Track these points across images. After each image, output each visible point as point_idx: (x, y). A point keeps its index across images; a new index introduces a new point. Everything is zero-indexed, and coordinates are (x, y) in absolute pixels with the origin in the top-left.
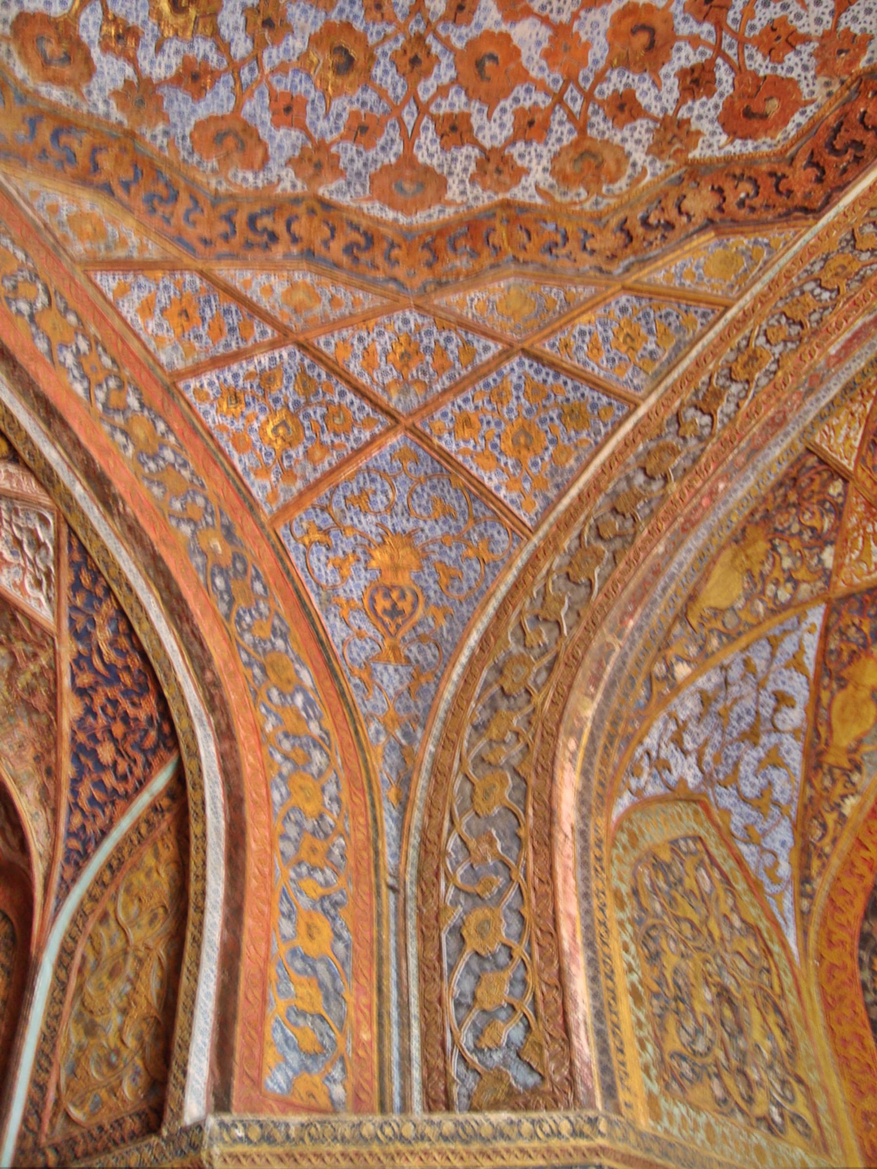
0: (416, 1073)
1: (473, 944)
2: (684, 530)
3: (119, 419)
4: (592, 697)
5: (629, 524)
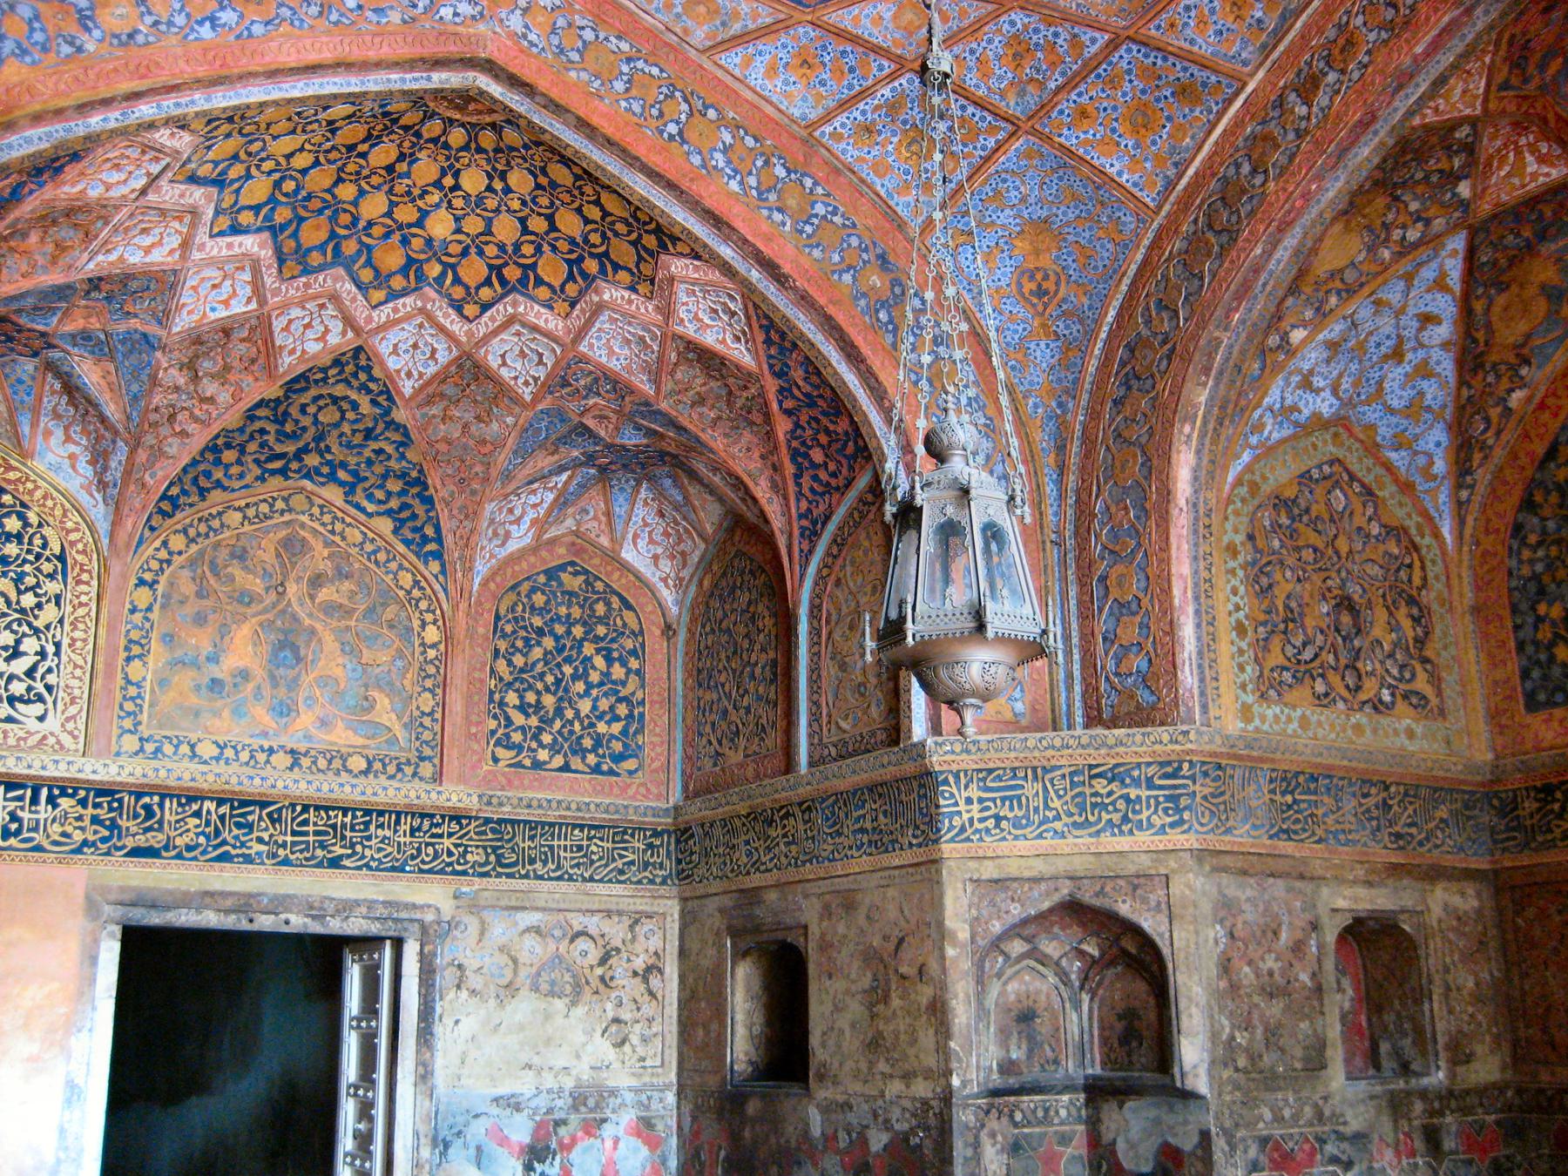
0: (1077, 688)
1: (1114, 593)
2: (1280, 230)
3: (772, 197)
4: (1205, 384)
5: (1234, 219)
